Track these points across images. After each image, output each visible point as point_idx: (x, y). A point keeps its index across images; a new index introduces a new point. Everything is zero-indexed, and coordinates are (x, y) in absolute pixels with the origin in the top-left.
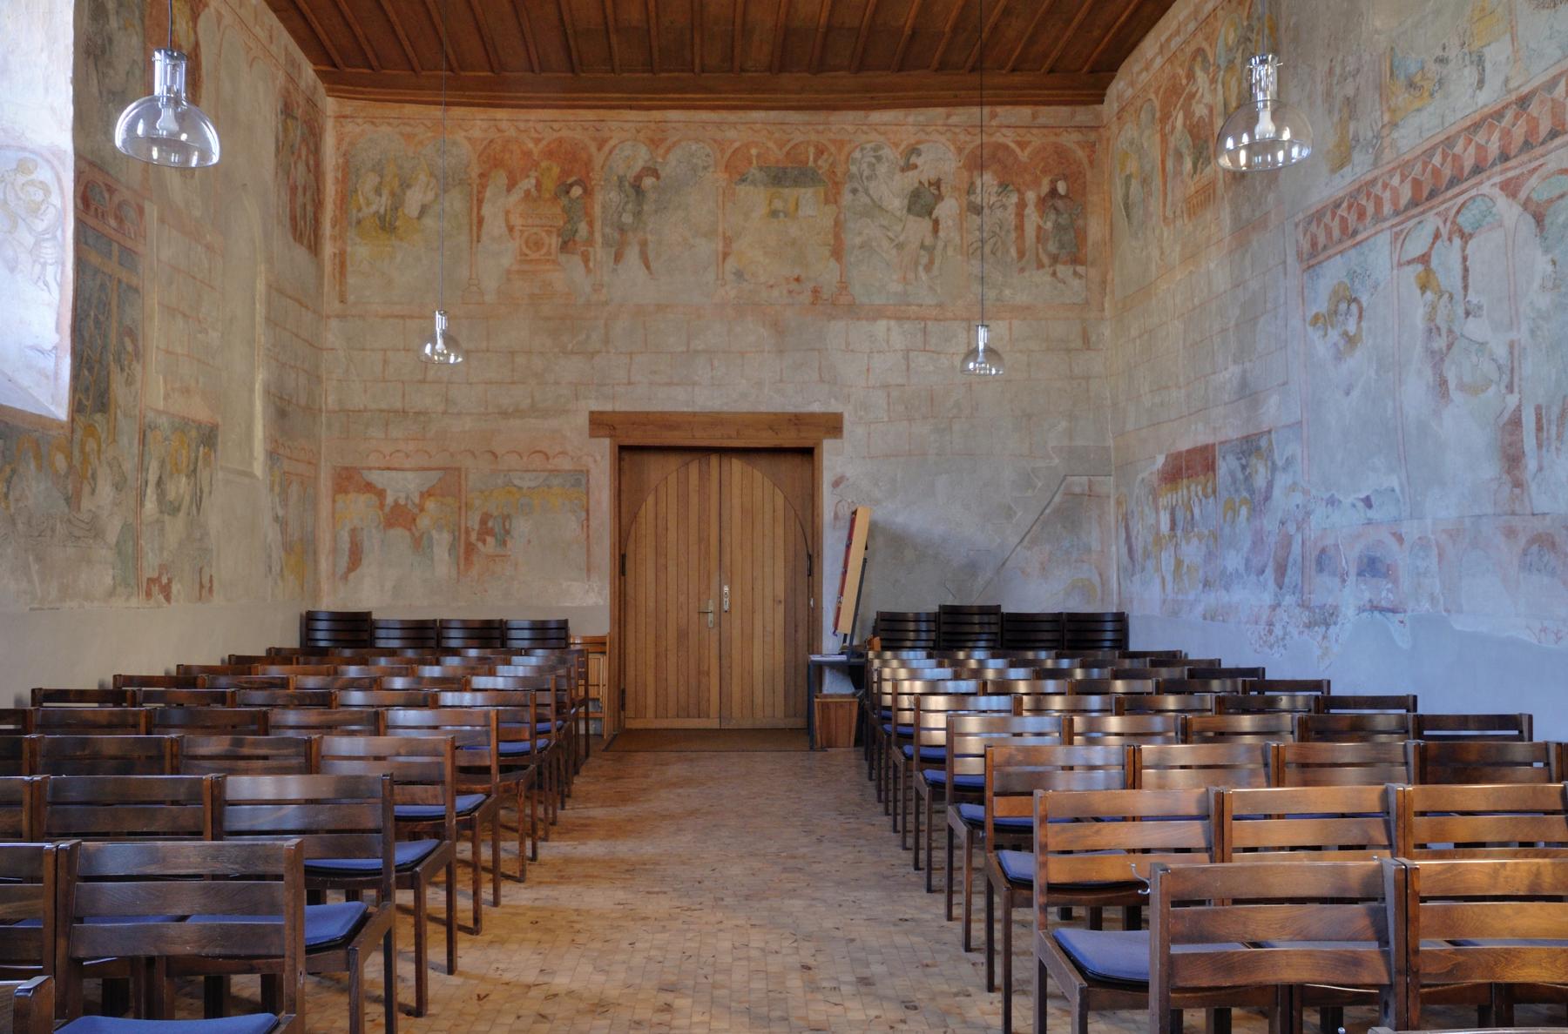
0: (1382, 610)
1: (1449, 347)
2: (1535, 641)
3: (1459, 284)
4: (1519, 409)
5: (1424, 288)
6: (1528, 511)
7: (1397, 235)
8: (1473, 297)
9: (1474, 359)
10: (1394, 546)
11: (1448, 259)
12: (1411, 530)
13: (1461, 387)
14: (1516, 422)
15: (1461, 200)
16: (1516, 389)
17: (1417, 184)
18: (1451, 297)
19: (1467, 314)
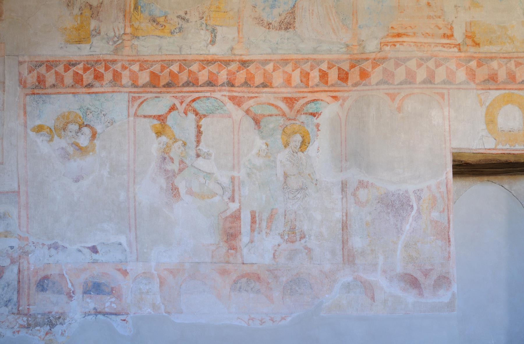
0: (105, 314)
1: (181, 170)
2: (246, 325)
3: (193, 138)
4: (239, 210)
5: (159, 134)
6: (240, 261)
7: (134, 99)
8: (203, 147)
9: (202, 181)
10: (119, 276)
11: (183, 125)
12: (135, 268)
13: (190, 192)
14: (236, 217)
15: (196, 95)
16: (237, 200)
17: (153, 75)
18: (185, 144)
19: (198, 156)
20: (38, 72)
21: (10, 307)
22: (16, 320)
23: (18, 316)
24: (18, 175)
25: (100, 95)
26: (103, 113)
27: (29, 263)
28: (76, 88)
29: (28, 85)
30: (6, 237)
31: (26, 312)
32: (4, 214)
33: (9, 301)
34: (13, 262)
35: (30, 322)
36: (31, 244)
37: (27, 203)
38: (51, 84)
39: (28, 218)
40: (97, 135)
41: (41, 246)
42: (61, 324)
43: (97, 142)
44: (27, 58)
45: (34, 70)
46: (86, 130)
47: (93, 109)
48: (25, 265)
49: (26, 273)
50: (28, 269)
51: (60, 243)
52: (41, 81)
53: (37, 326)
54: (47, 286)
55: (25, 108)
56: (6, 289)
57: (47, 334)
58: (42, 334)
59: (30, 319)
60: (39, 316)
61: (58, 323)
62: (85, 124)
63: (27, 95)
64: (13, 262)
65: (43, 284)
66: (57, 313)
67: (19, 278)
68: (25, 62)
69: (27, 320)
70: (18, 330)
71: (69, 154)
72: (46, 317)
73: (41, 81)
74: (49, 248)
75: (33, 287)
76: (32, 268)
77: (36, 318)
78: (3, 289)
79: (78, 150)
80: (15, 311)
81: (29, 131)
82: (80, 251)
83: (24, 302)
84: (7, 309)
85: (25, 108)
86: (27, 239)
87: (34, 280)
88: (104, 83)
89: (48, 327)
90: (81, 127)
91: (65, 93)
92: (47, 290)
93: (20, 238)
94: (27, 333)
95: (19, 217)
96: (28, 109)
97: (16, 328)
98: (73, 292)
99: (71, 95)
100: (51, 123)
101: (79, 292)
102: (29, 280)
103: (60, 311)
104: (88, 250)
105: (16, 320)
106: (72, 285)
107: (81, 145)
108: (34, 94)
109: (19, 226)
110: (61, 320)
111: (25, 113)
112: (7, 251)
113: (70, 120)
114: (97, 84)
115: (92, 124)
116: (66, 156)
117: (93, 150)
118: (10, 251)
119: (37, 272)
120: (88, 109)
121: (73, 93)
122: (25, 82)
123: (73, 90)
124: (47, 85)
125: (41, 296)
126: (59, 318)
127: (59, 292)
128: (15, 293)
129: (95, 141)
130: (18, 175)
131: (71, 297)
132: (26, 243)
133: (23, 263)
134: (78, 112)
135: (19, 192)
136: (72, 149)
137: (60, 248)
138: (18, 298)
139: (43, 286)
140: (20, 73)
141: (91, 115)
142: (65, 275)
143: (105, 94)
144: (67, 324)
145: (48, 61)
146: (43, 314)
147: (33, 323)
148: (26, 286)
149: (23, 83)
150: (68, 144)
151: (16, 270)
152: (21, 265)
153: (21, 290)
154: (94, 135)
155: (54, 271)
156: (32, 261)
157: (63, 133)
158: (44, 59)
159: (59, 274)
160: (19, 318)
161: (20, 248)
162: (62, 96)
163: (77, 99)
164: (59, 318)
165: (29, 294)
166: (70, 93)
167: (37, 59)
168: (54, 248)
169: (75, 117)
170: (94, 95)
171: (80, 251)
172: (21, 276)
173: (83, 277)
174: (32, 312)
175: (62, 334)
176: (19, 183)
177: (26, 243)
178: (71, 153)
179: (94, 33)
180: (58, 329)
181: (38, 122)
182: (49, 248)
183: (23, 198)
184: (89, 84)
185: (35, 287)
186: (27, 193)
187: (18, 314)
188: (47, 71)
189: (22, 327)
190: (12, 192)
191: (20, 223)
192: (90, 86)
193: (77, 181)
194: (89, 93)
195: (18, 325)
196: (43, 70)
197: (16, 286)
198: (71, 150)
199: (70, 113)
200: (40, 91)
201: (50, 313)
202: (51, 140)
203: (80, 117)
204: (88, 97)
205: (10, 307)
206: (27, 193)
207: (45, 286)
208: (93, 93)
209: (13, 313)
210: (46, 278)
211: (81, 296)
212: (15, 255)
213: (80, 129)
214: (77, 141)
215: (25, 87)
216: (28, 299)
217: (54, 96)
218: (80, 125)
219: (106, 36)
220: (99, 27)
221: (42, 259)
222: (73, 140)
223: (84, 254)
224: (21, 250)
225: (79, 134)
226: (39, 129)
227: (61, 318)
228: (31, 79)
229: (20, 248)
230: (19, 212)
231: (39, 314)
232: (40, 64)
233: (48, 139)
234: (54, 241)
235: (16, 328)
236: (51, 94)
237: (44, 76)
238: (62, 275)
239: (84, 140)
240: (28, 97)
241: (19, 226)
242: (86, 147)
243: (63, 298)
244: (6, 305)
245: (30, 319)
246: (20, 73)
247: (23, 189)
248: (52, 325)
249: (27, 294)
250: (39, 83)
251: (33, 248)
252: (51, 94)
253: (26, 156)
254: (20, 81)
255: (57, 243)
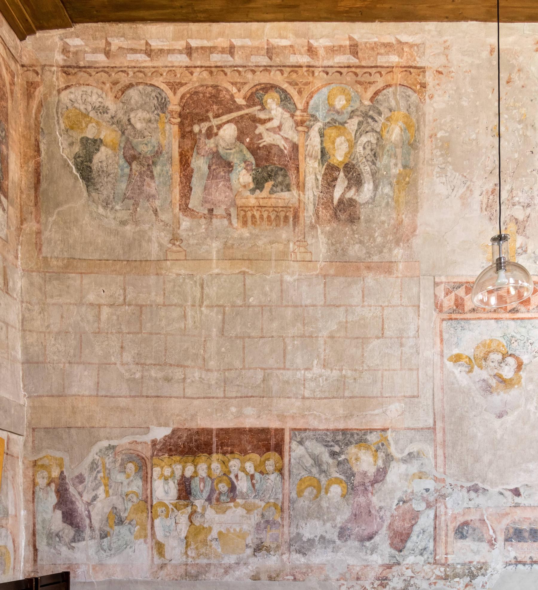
20: (456, 294)
21: (426, 556)
22: (432, 570)
23: (435, 566)
24: (434, 409)
25: (527, 321)
26: (530, 341)
27: (446, 507)
28: (498, 313)
29: (445, 309)
30: (420, 478)
31: (443, 561)
32: (418, 453)
33: (425, 549)
34: (429, 506)
35: (448, 573)
36: (448, 486)
37: (444, 441)
38: (470, 308)
39: (445, 457)
40: (523, 367)
41: (460, 488)
42: (483, 575)
43: (522, 374)
44: (443, 279)
45: (451, 292)
46: (511, 360)
47: (518, 336)
48: (442, 509)
49: (443, 518)
50: (446, 514)
51: (481, 485)
52: (459, 305)
53: (455, 577)
54: (467, 533)
55: (441, 335)
56: (421, 536)
57: (466, 586)
58: (462, 586)
59: (448, 569)
60: (459, 566)
61: (480, 574)
62: (509, 353)
63: (443, 320)
64: (429, 506)
65: (462, 531)
66: (478, 562)
67: (435, 524)
68: (442, 283)
69: (445, 571)
70: (434, 581)
71: (491, 387)
72: (467, 567)
73: (459, 305)
74: (468, 491)
75: (451, 534)
76: (450, 512)
77: (455, 568)
78: (418, 537)
79: (501, 382)
80: (431, 560)
81: (445, 360)
82: (501, 494)
83: (441, 550)
84: (422, 559)
85: (441, 335)
86: (444, 480)
87: (451, 527)
88: (531, 308)
89: (469, 579)
90: (505, 356)
91: (486, 319)
92: (466, 537)
93: (436, 479)
94: (444, 585)
95: (435, 457)
96: (446, 336)
97: (432, 580)
98: (495, 539)
99: (493, 321)
100: (470, 352)
101: (501, 538)
102: (447, 526)
103: (483, 561)
104: (510, 493)
105: (432, 570)
106: (494, 532)
107: (505, 377)
108: (451, 319)
109: (436, 466)
110: (483, 571)
111: (442, 340)
112: (422, 494)
113: (492, 349)
114: (522, 308)
115: (517, 353)
116: (488, 389)
117: (519, 382)
118: (425, 494)
119: (456, 518)
120: (512, 337)
121: (495, 319)
122: (441, 306)
123: (495, 316)
124: (467, 309)
125: (460, 543)
126: (481, 568)
127: (480, 540)
128: (432, 540)
129: (521, 373)
130: (434, 409)
131: (493, 545)
132: (443, 484)
133: (439, 507)
134: (501, 340)
135: (434, 429)
136: (494, 381)
137: (481, 491)
138: (435, 546)
139: (462, 533)
140: (435, 296)
141: (516, 344)
142: (486, 520)
143: (532, 321)
144: (489, 575)
145: (467, 283)
146: (463, 564)
147: (452, 574)
148: (443, 533)
149: (439, 307)
150: (490, 375)
151: (432, 516)
152: (438, 510)
153: (437, 538)
154: (520, 366)
155: (473, 516)
156: (449, 506)
157: (484, 363)
158: (463, 280)
159: (480, 520)
160: (436, 568)
161: (436, 490)
162: (483, 322)
163: (500, 325)
164: (481, 568)
165: (446, 542)
166: (492, 319)
167: (455, 280)
168: (474, 490)
169: (498, 346)
170: (519, 321)
171: (501, 494)
172: (437, 522)
173: (506, 522)
174: (450, 562)
175: (483, 586)
176: (434, 418)
177: (443, 484)
178: (494, 385)
179: (520, 251)
180: (479, 580)
181: (456, 351)
182: (468, 491)
183: (439, 436)
184: (514, 309)
185: (453, 534)
186: (444, 429)
187: (434, 564)
188: (467, 293)
189: (439, 578)
190: (426, 428)
191: (436, 463)
192: (514, 311)
193: (500, 416)
194: (513, 319)
195: (434, 576)
196: (461, 292)
197: (432, 533)
198: (493, 382)
199: (491, 341)
200: (459, 316)
201: (470, 562)
202: (470, 371)
203: (503, 346)
204: (512, 323)
205: (426, 556)
206: (444, 429)
207: (465, 533)
208: (518, 319)
209: (429, 563)
210: (466, 523)
211: (503, 543)
212: (431, 499)
213: (503, 359)
214: (500, 372)
215: (441, 311)
216: (446, 548)
217: (474, 322)
218: (503, 355)
219: (533, 255)
220: (526, 245)
221: (460, 503)
222: (496, 371)
223: (506, 497)
224: (438, 493)
225: (502, 365)
226: (457, 359)
227: (482, 568)
228: (448, 302)
229: (436, 490)
230: (435, 451)
231: (459, 564)
232: (460, 285)
233: (467, 370)
234: (473, 483)
235: (432, 580)
236: (470, 319)
237: (462, 299)
238: (482, 521)
239: (508, 372)
240: (445, 322)
241: (436, 466)
242: (511, 380)
243: (485, 546)
244: (421, 554)
245: (448, 569)
246: (435, 296)
247: (439, 425)
248: (473, 576)
249: (444, 541)
250: (457, 307)
251: (451, 490)
252: (470, 319)
253: (442, 389)
254: (436, 305)
255: (477, 485)
